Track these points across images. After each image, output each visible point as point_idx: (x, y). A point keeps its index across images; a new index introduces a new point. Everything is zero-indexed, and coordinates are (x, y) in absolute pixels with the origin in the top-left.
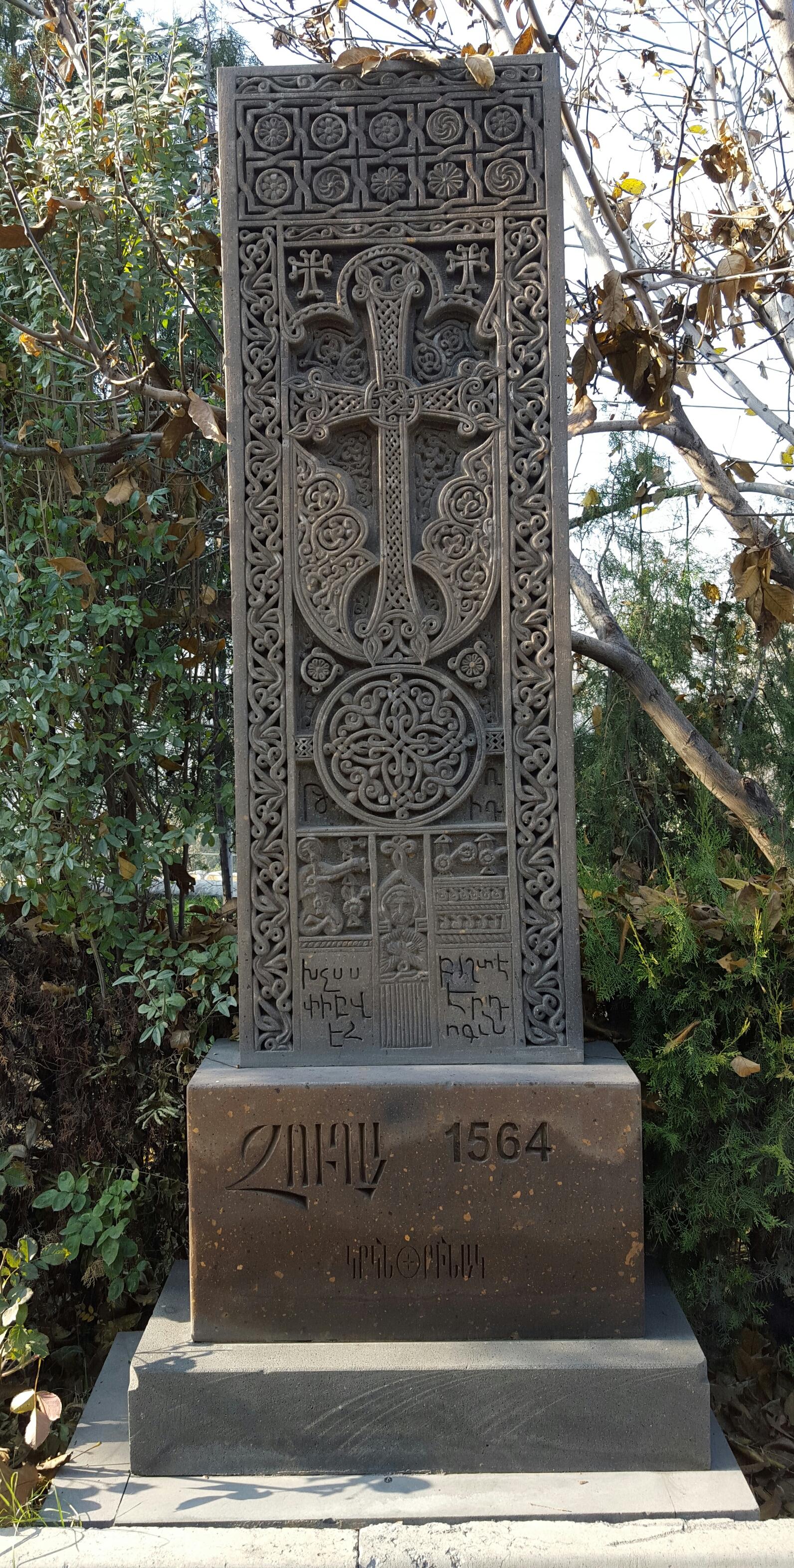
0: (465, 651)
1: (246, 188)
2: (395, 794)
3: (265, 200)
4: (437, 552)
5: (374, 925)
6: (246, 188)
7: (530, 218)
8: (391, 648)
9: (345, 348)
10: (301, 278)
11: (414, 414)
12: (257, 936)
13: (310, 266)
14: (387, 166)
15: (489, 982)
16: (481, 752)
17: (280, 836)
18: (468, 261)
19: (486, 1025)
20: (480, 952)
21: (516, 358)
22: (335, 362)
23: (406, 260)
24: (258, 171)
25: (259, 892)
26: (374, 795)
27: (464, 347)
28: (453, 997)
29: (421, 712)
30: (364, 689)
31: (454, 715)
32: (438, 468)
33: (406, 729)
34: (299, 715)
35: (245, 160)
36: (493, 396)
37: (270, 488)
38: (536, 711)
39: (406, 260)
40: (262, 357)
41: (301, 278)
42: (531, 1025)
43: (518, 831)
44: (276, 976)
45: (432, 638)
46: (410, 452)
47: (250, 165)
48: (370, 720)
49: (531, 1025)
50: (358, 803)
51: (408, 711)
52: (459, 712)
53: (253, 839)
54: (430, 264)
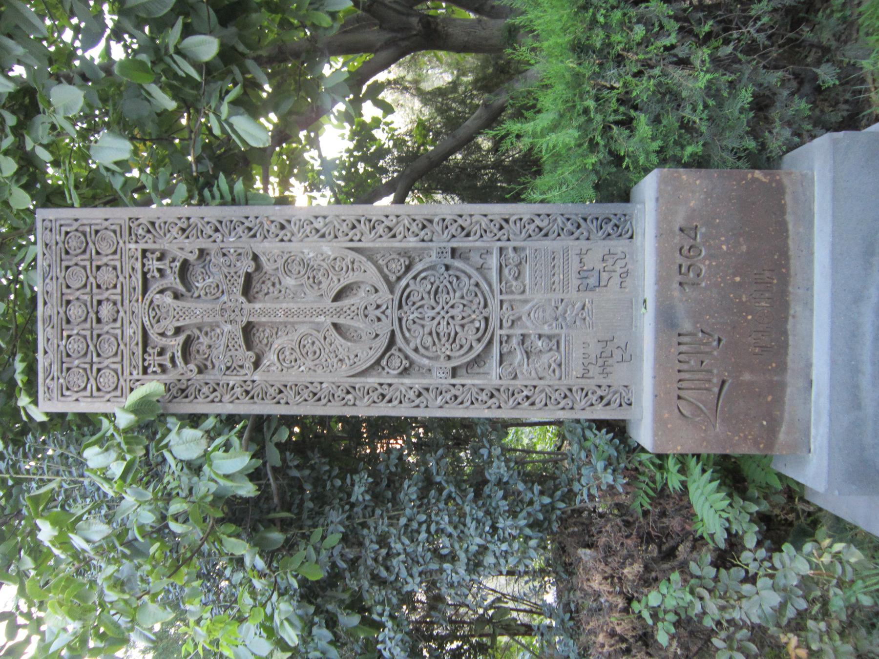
0: (385, 270)
1: (108, 396)
2: (474, 316)
3: (114, 386)
4: (324, 286)
5: (556, 331)
6: (108, 396)
7: (130, 228)
8: (383, 317)
9: (201, 340)
10: (160, 365)
11: (242, 299)
12: (561, 406)
13: (153, 360)
14: (97, 312)
15: (593, 261)
16: (449, 261)
17: (499, 390)
18: (153, 265)
19: (620, 263)
20: (575, 265)
21: (210, 236)
22: (210, 347)
23: (152, 302)
24: (99, 389)
25: (533, 404)
26: (474, 331)
27: (204, 267)
28: (602, 284)
29: (423, 298)
30: (407, 334)
31: (424, 278)
32: (274, 285)
33: (433, 308)
34: (423, 375)
35: (92, 396)
36: (232, 251)
37: (283, 389)
38: (424, 227)
39: (152, 302)
40: (205, 389)
41: (160, 365)
43: (499, 240)
44: (586, 395)
45: (376, 291)
46: (265, 302)
47: (95, 393)
48: (427, 330)
49: (620, 235)
50: (479, 340)
51: (421, 306)
52: (423, 275)
53: (500, 407)
54: (154, 287)
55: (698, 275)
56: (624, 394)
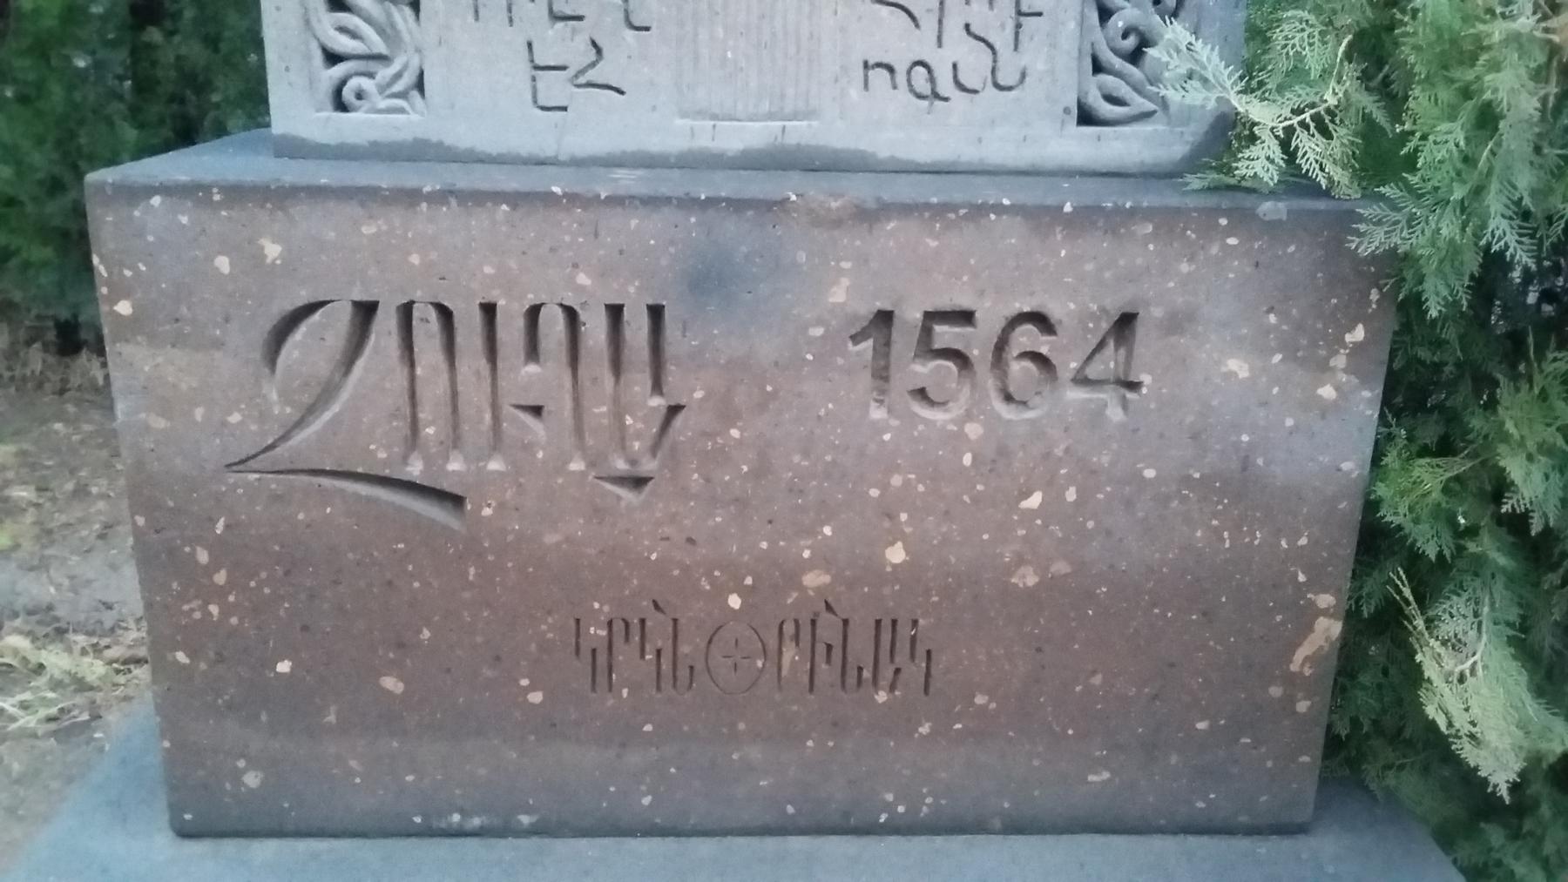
19: (975, 64)
42: (1098, 68)
49: (1098, 68)
55: (921, 394)
56: (385, 73)
